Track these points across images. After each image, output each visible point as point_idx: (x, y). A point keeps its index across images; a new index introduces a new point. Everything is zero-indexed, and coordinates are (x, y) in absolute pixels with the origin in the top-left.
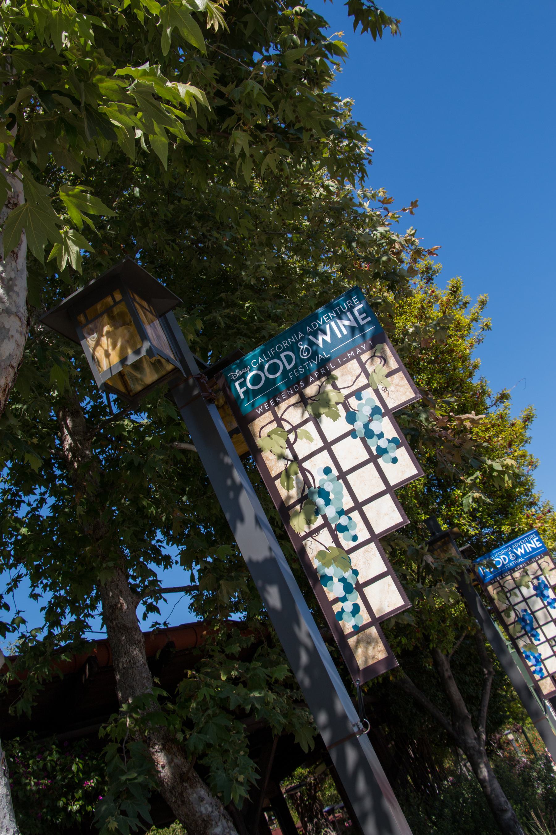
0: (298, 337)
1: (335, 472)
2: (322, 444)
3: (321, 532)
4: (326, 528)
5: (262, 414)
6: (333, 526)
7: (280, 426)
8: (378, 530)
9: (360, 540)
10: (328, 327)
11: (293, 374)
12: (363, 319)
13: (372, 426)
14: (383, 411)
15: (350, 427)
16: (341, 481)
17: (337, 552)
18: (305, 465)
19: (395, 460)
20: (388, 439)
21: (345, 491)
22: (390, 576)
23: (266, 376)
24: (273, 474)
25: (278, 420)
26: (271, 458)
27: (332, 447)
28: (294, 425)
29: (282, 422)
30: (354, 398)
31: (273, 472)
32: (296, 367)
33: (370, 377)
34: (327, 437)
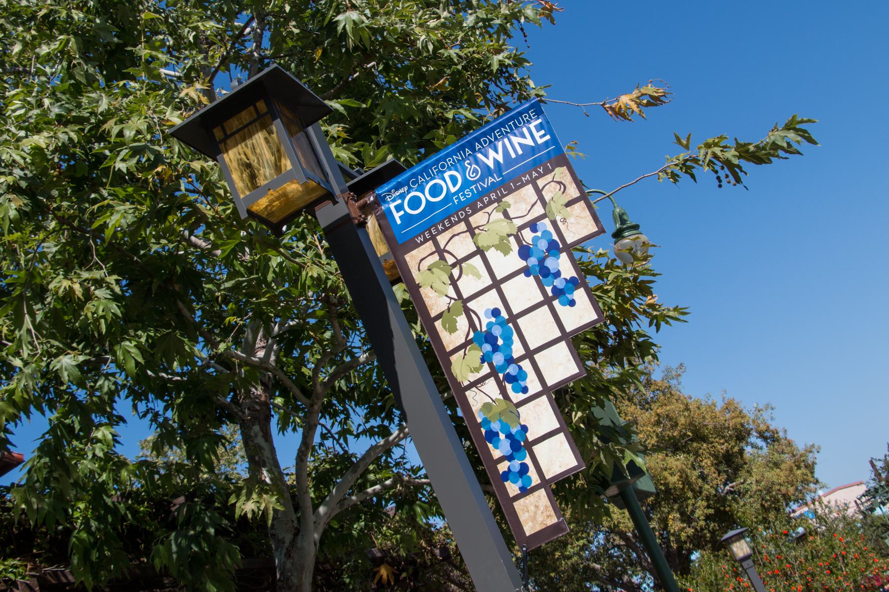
0: (465, 155)
1: (504, 314)
2: (490, 282)
3: (487, 381)
4: (493, 378)
5: (422, 243)
6: (501, 376)
7: (442, 258)
8: (551, 381)
9: (531, 392)
11: (458, 198)
12: (541, 137)
13: (550, 263)
14: (561, 246)
15: (522, 264)
16: (511, 325)
17: (504, 405)
18: (471, 305)
19: (572, 303)
20: (565, 279)
21: (515, 337)
22: (562, 434)
23: (423, 193)
24: (433, 314)
25: (441, 252)
26: (431, 295)
27: (502, 286)
28: (459, 258)
29: (445, 254)
30: (528, 229)
31: (433, 311)
33: (547, 206)
34: (496, 274)
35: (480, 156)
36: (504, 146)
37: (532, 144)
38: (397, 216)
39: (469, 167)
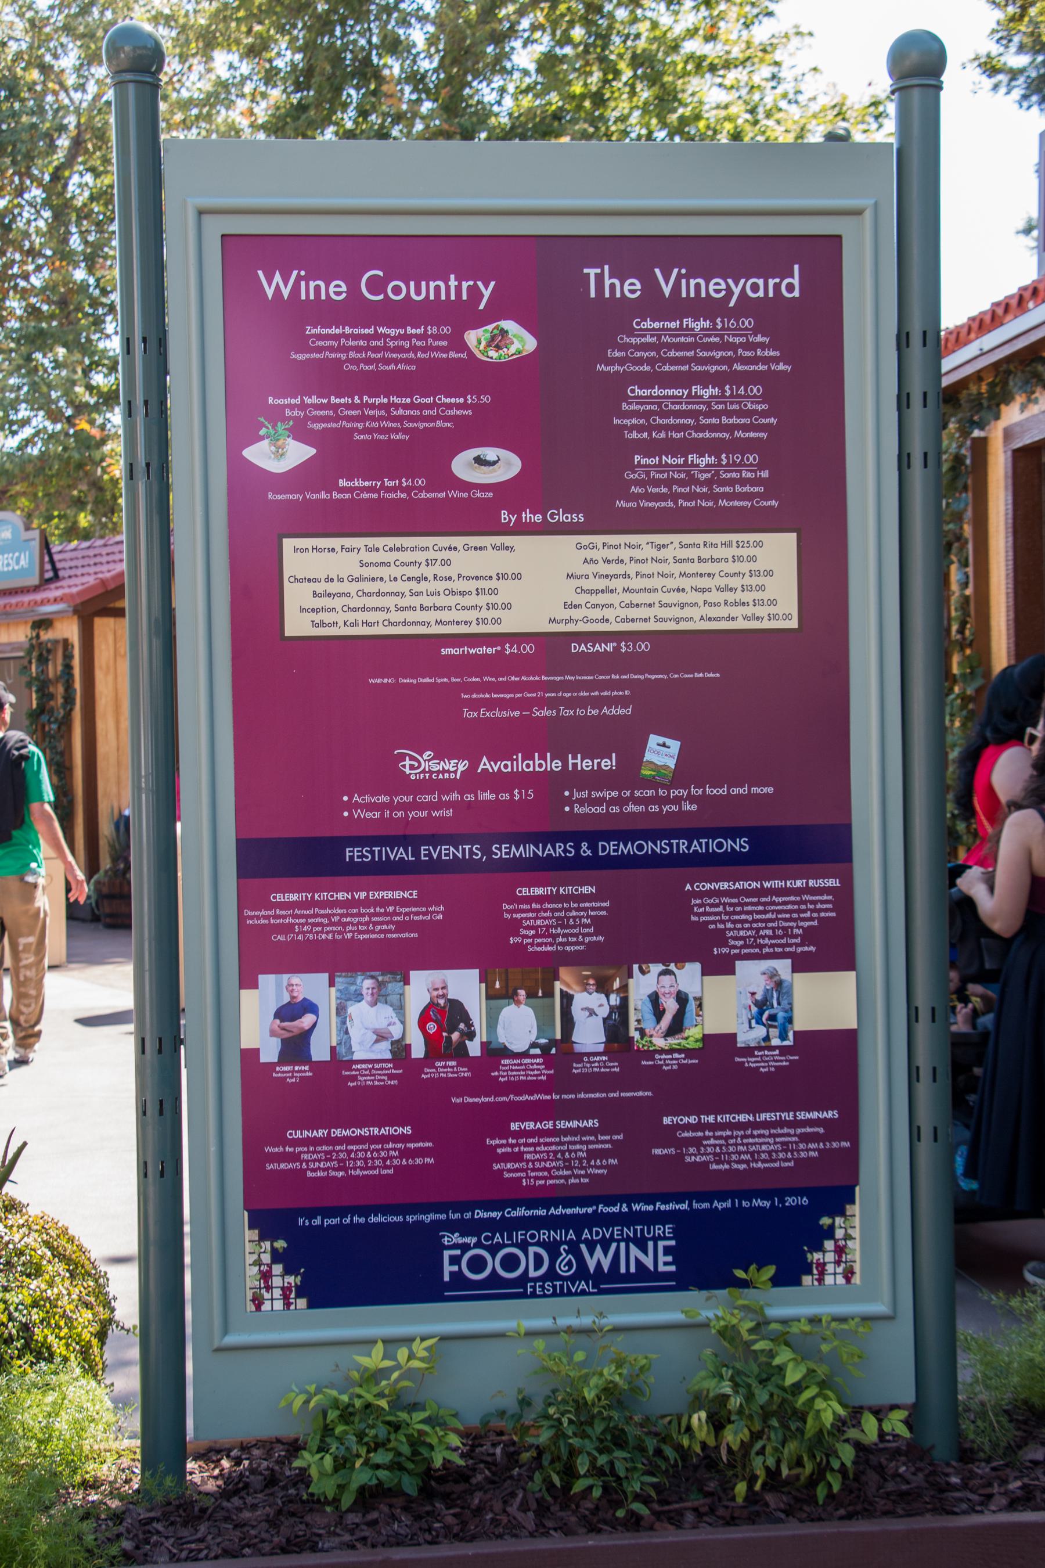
10: (614, 1245)
11: (534, 1287)
12: (666, 1264)
32: (543, 1279)
35: (583, 1247)
36: (618, 1248)
37: (652, 1268)
38: (448, 1269)
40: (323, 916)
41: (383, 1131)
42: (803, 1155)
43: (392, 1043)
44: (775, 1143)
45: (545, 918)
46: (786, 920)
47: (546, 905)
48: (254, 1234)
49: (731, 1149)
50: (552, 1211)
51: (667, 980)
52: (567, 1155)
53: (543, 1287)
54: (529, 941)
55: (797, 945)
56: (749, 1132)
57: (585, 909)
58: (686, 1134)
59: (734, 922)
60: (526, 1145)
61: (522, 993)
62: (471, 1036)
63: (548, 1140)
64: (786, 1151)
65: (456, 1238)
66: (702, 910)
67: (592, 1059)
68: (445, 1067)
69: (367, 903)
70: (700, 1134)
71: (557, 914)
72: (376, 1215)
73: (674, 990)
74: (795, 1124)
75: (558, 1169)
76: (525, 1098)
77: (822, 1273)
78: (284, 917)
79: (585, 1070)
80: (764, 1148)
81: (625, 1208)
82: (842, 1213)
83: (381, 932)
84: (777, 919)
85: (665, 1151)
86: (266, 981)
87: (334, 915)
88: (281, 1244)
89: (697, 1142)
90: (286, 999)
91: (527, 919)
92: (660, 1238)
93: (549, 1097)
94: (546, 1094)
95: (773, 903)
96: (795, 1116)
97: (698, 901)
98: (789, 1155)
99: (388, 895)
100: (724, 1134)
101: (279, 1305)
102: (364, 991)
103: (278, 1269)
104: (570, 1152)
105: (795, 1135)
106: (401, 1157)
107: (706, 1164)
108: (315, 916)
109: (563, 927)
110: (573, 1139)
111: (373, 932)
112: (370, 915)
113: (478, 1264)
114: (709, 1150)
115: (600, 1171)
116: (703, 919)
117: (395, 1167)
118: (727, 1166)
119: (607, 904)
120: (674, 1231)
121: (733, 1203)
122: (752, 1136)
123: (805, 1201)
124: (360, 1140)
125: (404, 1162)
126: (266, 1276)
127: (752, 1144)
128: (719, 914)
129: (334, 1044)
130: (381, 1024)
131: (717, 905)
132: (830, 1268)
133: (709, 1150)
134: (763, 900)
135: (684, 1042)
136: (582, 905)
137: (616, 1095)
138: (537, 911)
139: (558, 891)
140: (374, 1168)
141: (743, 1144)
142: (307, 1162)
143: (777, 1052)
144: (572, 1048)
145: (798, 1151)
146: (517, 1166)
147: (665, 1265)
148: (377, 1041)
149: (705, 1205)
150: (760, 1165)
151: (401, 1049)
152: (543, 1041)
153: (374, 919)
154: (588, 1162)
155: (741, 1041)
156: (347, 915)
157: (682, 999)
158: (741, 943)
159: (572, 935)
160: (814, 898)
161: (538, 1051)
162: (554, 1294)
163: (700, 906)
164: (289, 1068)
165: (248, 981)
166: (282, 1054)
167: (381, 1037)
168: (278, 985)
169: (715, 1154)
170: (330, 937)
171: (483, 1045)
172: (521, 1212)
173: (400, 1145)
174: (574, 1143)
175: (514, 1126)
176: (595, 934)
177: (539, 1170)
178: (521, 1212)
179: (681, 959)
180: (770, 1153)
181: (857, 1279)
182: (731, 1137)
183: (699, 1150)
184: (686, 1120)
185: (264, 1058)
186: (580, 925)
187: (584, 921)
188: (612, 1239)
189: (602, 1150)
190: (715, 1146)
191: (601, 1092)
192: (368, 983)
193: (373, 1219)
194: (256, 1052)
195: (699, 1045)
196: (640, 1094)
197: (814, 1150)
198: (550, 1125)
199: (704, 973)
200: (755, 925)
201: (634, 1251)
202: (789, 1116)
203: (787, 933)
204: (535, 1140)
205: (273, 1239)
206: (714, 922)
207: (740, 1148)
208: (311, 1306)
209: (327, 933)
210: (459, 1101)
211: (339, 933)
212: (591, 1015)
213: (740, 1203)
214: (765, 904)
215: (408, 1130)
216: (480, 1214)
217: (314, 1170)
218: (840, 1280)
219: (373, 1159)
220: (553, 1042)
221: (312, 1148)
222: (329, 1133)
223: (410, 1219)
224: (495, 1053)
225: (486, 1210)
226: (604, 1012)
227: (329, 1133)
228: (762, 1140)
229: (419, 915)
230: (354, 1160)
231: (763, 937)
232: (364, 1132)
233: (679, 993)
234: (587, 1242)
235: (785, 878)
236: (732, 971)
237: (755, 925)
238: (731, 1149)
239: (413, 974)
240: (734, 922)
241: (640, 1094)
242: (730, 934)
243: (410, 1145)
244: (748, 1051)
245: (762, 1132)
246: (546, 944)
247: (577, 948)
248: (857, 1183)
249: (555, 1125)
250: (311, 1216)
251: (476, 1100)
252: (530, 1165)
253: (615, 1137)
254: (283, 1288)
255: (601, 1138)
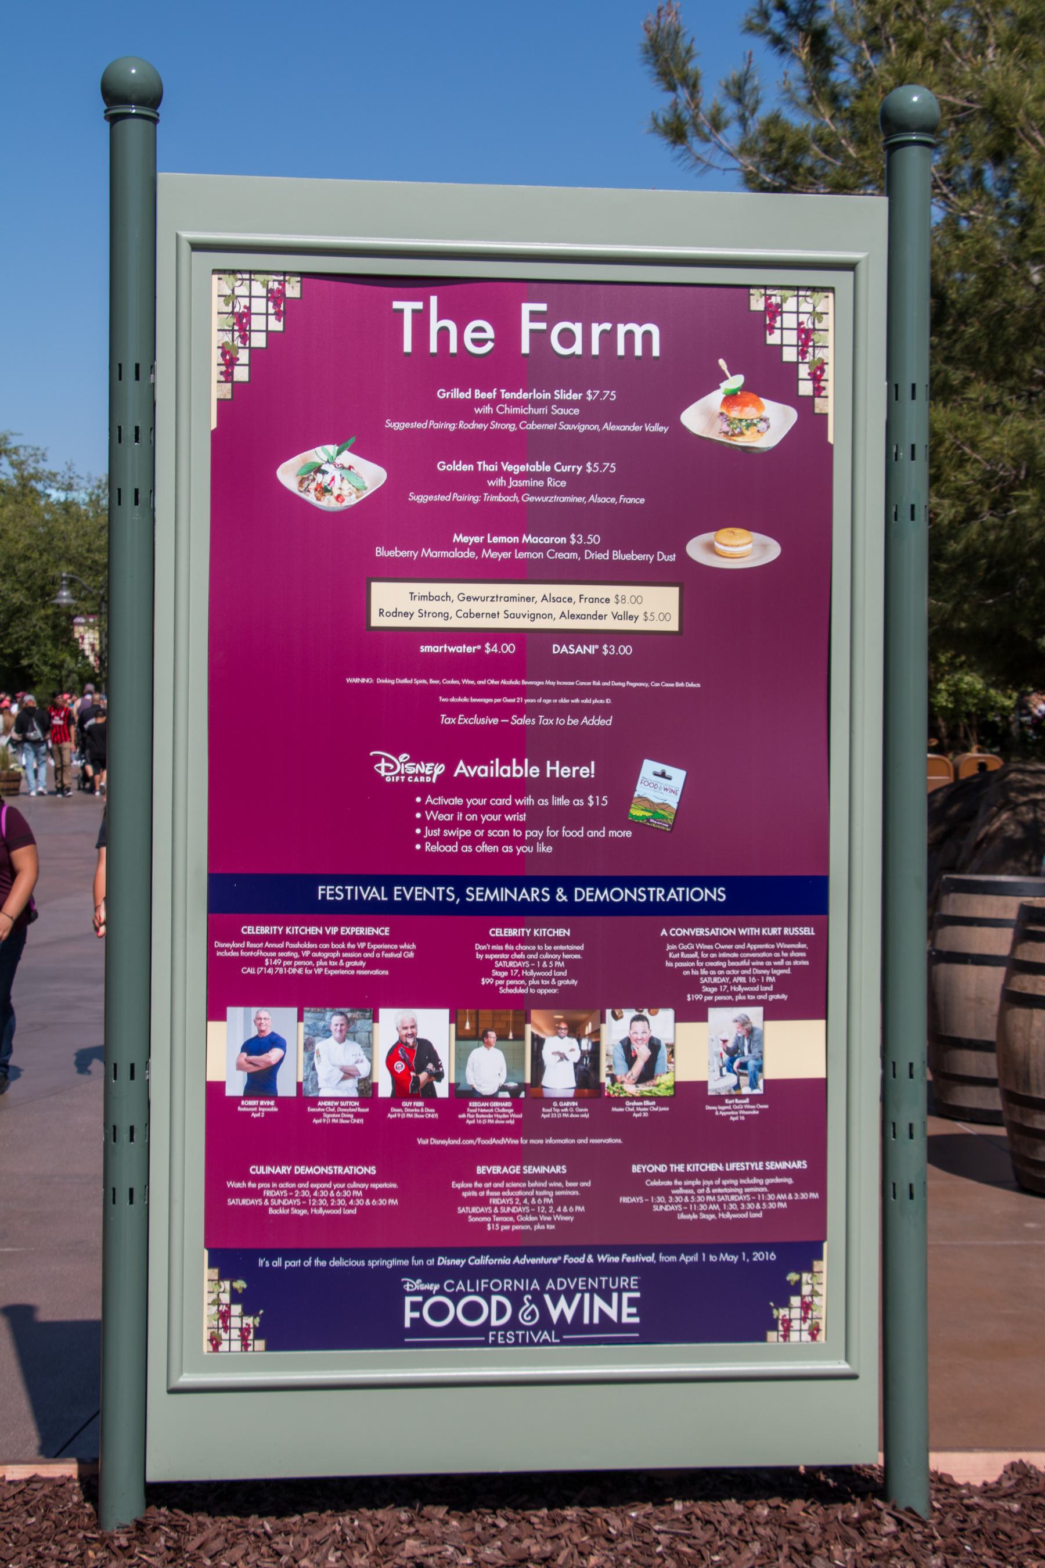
10: (578, 1296)
11: (496, 1336)
12: (630, 1315)
32: (505, 1328)
35: (547, 1297)
38: (409, 1315)
39: (528, 1304)
40: (293, 950)
41: (347, 1170)
42: (772, 1206)
43: (360, 1081)
44: (744, 1193)
45: (518, 960)
46: (760, 968)
47: (520, 947)
48: (215, 1273)
49: (700, 1199)
50: (517, 1260)
51: (639, 1025)
52: (533, 1201)
53: (505, 1336)
54: (501, 982)
55: (769, 993)
56: (718, 1182)
57: (559, 952)
58: (654, 1183)
59: (709, 969)
60: (492, 1189)
61: (492, 1035)
62: (439, 1076)
63: (514, 1185)
64: (755, 1202)
65: (419, 1285)
66: (677, 956)
67: (561, 1104)
68: (412, 1107)
69: (338, 938)
70: (669, 1183)
71: (530, 956)
72: (337, 1259)
73: (646, 1036)
74: (765, 1174)
75: (524, 1214)
76: (492, 1141)
77: (787, 1329)
78: (255, 950)
79: (554, 1116)
80: (733, 1198)
81: (590, 1259)
82: (810, 1269)
83: (351, 968)
84: (752, 967)
85: (633, 1200)
86: (235, 1013)
87: (305, 949)
88: (240, 1285)
89: (666, 1191)
90: (254, 1033)
91: (499, 960)
92: (625, 1290)
93: (516, 1142)
94: (514, 1138)
95: (748, 951)
96: (764, 1166)
97: (674, 947)
98: (758, 1206)
99: (360, 931)
100: (693, 1183)
101: (237, 1346)
102: (333, 1028)
103: (237, 1309)
104: (537, 1197)
105: (764, 1186)
106: (364, 1197)
107: (674, 1213)
108: (285, 950)
109: (536, 969)
110: (540, 1185)
111: (344, 968)
112: (341, 951)
113: (439, 1311)
114: (678, 1199)
115: (567, 1218)
116: (678, 965)
117: (359, 1208)
118: (695, 1216)
119: (581, 948)
120: (640, 1283)
121: (700, 1257)
122: (721, 1186)
123: (773, 1257)
124: (323, 1178)
125: (368, 1202)
126: (225, 1316)
127: (721, 1194)
128: (694, 960)
129: (301, 1080)
130: (348, 1061)
131: (692, 952)
132: (796, 1324)
133: (678, 1199)
134: (738, 947)
135: (655, 1090)
136: (556, 948)
137: (585, 1141)
138: (510, 952)
139: (532, 933)
140: (336, 1207)
141: (712, 1194)
142: (269, 1198)
143: (747, 1101)
144: (542, 1092)
145: (767, 1202)
146: (482, 1210)
147: (629, 1316)
148: (344, 1079)
149: (672, 1258)
150: (728, 1216)
151: (368, 1090)
152: (512, 1085)
153: (345, 955)
154: (555, 1209)
155: (713, 1089)
156: (317, 950)
157: (654, 1046)
158: (715, 990)
159: (546, 978)
160: (789, 946)
161: (507, 1095)
162: (516, 1344)
163: (675, 952)
164: (254, 1103)
165: (216, 1012)
166: (248, 1088)
167: (348, 1074)
168: (247, 1018)
169: (683, 1204)
170: (300, 971)
171: (452, 1087)
172: (484, 1260)
173: (363, 1186)
174: (541, 1189)
175: (480, 1170)
176: (568, 977)
177: (504, 1215)
178: (484, 1260)
179: (655, 1004)
180: (738, 1203)
181: (821, 1337)
182: (700, 1187)
183: (667, 1199)
184: (655, 1168)
185: (230, 1092)
186: (554, 968)
187: (558, 964)
188: (576, 1290)
189: (569, 1196)
190: (683, 1195)
191: (570, 1138)
192: (337, 1019)
193: (335, 1263)
194: (221, 1086)
195: (671, 1092)
196: (610, 1141)
197: (783, 1201)
198: (516, 1170)
199: (678, 1019)
200: (729, 972)
201: (599, 1302)
202: (758, 1166)
203: (760, 980)
204: (501, 1185)
205: (233, 1278)
206: (689, 969)
207: (709, 1198)
208: (269, 1348)
209: (298, 967)
210: (425, 1142)
211: (310, 967)
212: (562, 1059)
213: (707, 1258)
214: (739, 951)
215: (372, 1170)
216: (444, 1261)
217: (275, 1207)
218: (806, 1337)
219: (336, 1198)
220: (523, 1086)
221: (274, 1185)
222: (292, 1170)
223: (372, 1264)
224: (462, 1096)
225: (450, 1257)
226: (576, 1057)
227: (292, 1170)
228: (730, 1190)
229: (390, 952)
230: (317, 1198)
231: (736, 985)
232: (328, 1170)
233: (652, 1039)
234: (551, 1292)
235: (760, 926)
236: (704, 1018)
237: (729, 972)
238: (700, 1199)
239: (383, 1012)
240: (709, 969)
241: (610, 1141)
242: (703, 981)
243: (375, 1186)
244: (719, 1099)
245: (731, 1181)
246: (518, 986)
247: (550, 991)
248: (824, 1239)
249: (522, 1170)
250: (271, 1255)
251: (443, 1142)
252: (496, 1210)
253: (583, 1184)
254: (241, 1329)
255: (569, 1184)
